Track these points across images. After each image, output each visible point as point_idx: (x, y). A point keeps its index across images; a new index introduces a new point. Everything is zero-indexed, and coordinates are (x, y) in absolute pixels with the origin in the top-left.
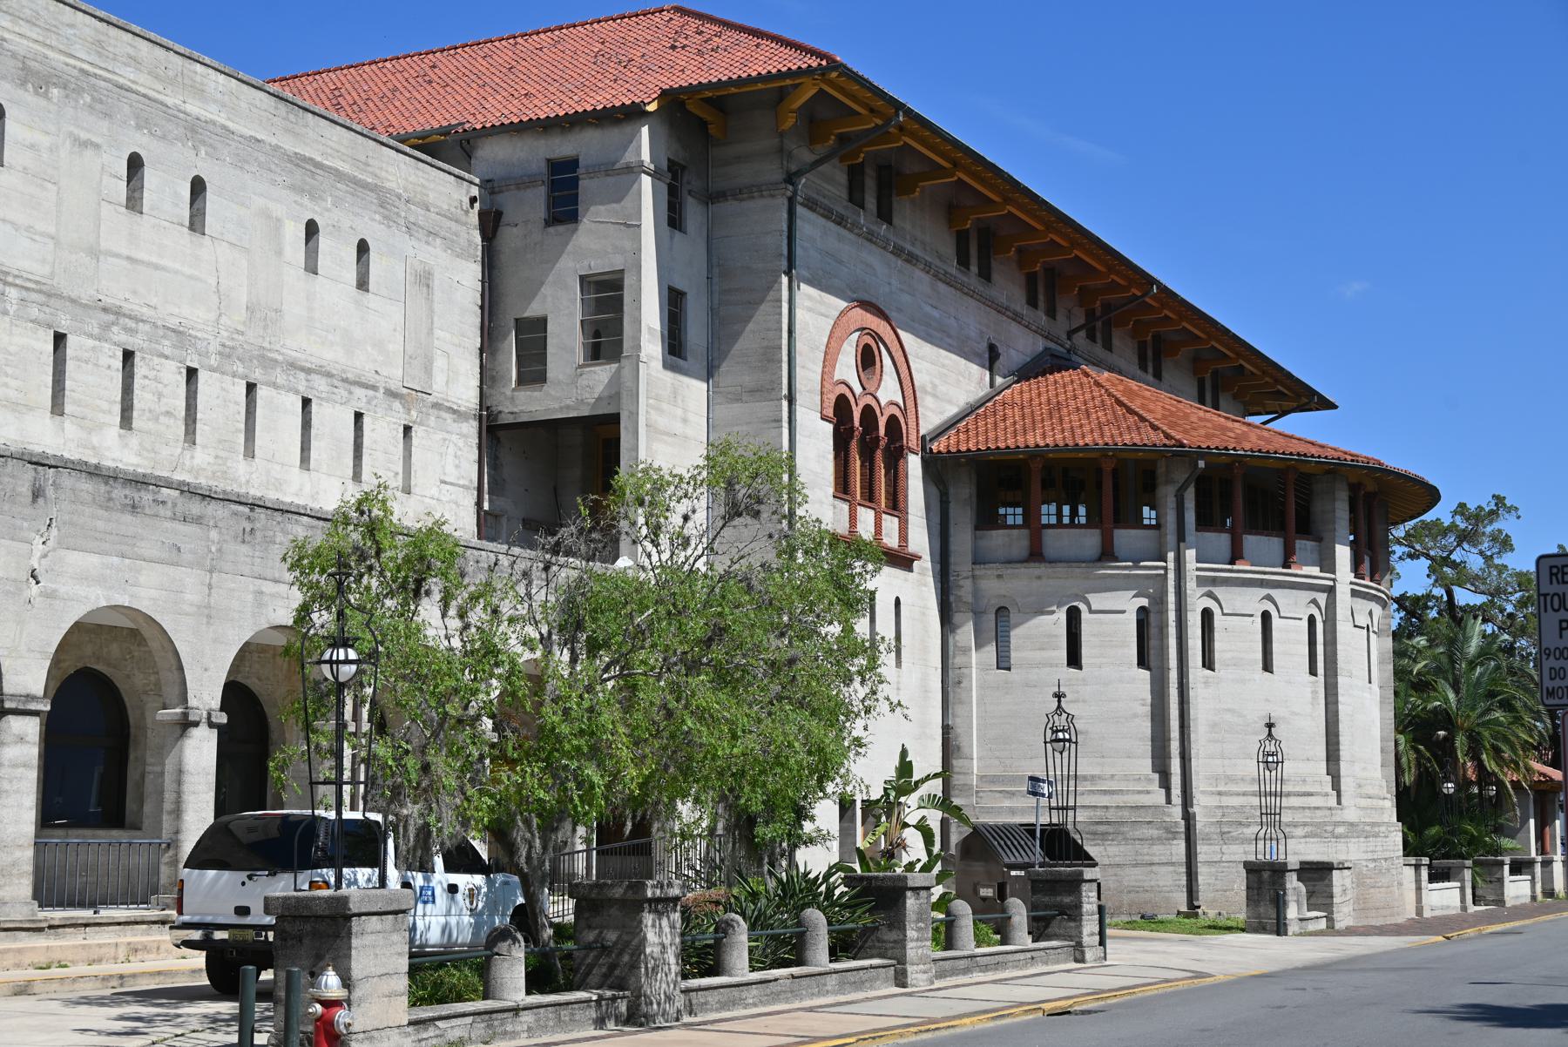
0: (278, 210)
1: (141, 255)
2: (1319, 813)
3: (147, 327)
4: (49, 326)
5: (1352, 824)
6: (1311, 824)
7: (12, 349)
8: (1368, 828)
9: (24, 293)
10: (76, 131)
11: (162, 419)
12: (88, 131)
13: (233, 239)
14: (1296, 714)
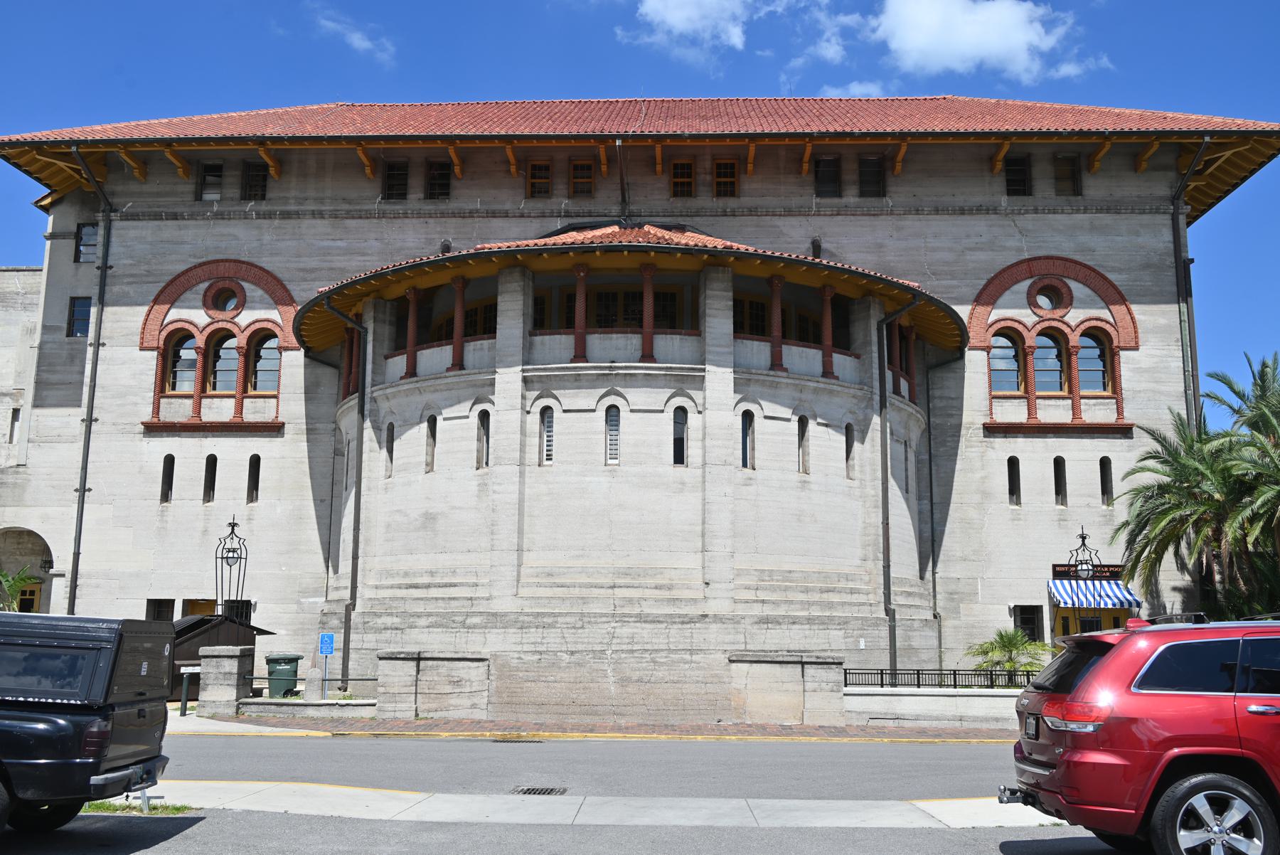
2: (454, 603)
5: (495, 615)
6: (437, 614)
8: (531, 618)
14: (454, 508)
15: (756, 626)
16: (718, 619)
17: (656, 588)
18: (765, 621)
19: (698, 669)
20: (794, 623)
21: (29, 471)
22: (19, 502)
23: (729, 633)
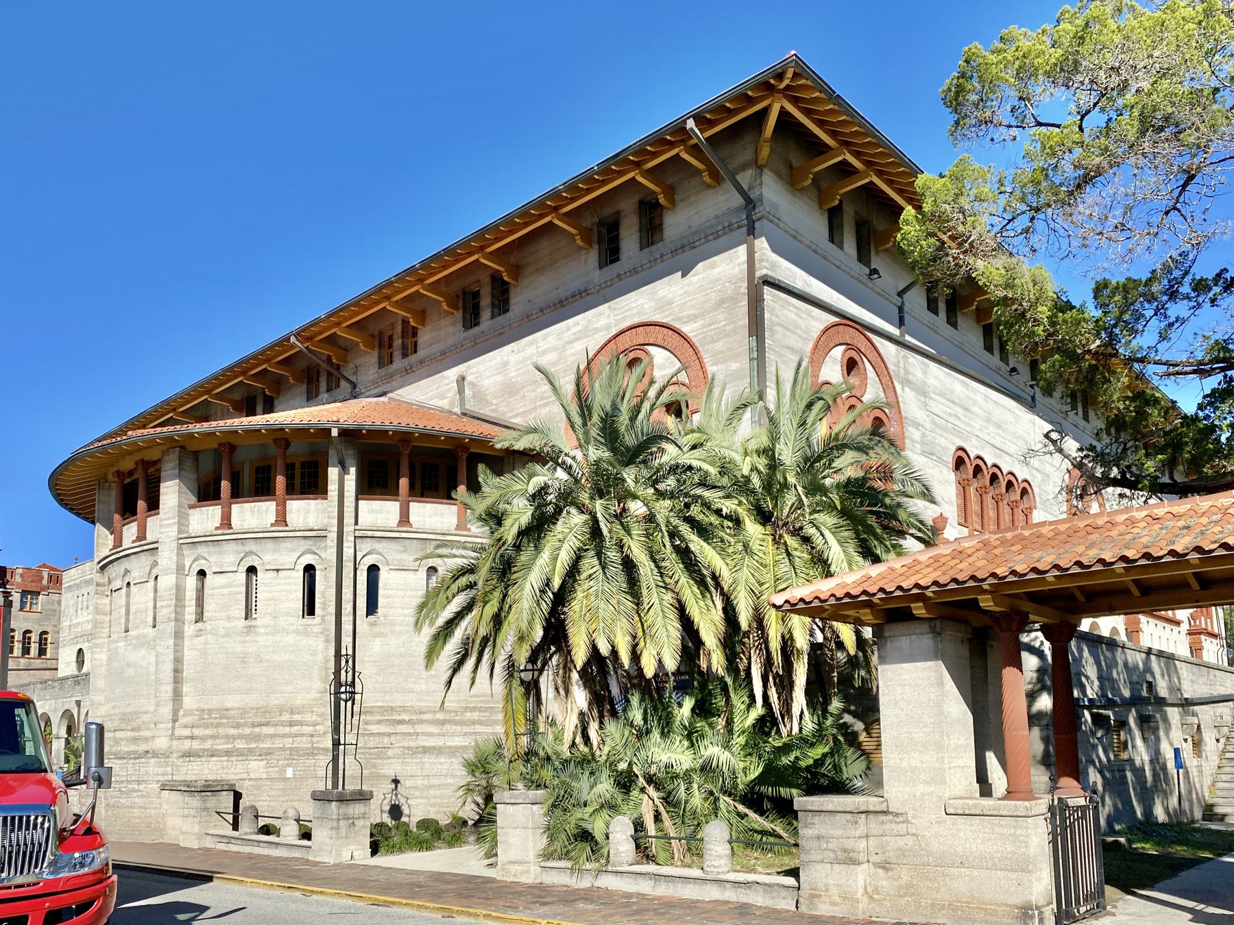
15: (181, 760)
16: (155, 754)
17: (132, 730)
18: (188, 754)
19: (142, 796)
20: (212, 756)
23: (161, 767)
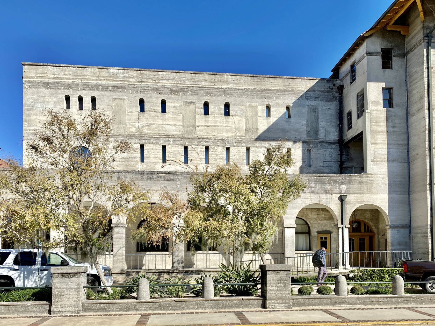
0: (254, 104)
1: (209, 124)
3: (212, 140)
4: (182, 145)
7: (171, 151)
9: (174, 139)
10: (187, 101)
11: (218, 160)
12: (191, 100)
13: (239, 114)
21: (373, 176)
22: (370, 192)
